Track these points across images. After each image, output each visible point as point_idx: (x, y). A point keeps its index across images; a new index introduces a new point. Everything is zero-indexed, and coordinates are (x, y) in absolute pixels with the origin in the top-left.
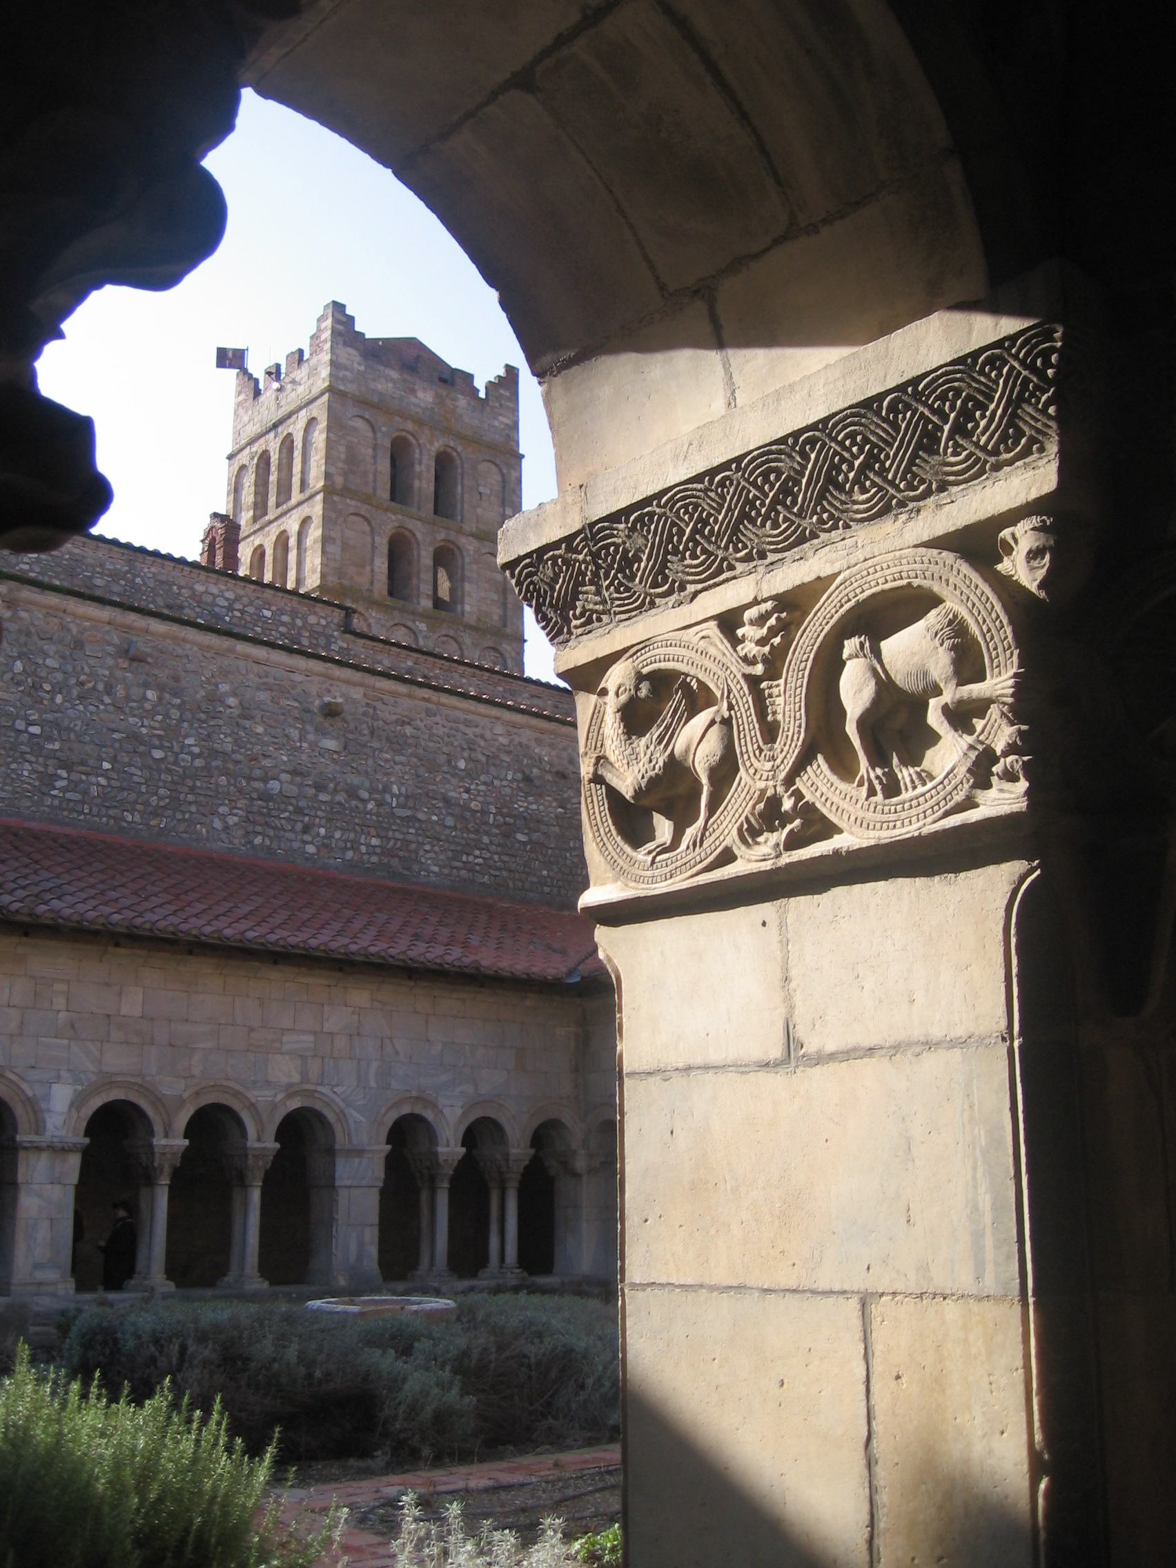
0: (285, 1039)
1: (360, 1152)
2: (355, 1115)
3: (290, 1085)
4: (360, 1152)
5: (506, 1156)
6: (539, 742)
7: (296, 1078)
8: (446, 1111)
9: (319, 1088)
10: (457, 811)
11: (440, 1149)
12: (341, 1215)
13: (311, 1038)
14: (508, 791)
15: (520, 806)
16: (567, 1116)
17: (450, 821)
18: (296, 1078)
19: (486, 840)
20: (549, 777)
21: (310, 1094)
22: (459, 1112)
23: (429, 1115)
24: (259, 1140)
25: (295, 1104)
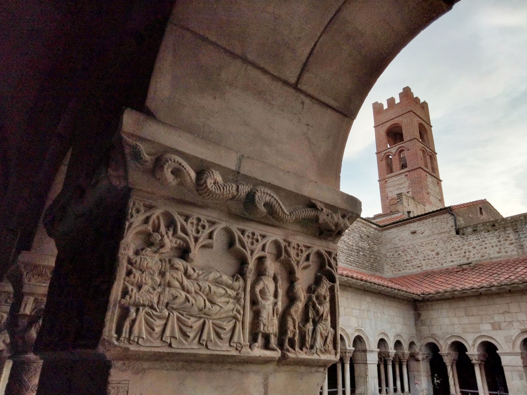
0: (353, 312)
1: (372, 351)
2: (371, 339)
3: (356, 327)
4: (372, 351)
5: (403, 354)
6: (362, 226)
7: (356, 325)
8: (390, 337)
9: (362, 329)
10: (347, 244)
11: (390, 351)
12: (369, 374)
13: (358, 311)
14: (357, 240)
15: (360, 244)
16: (415, 342)
17: (345, 247)
18: (356, 325)
19: (354, 253)
20: (366, 237)
21: (359, 330)
22: (393, 338)
23: (385, 338)
24: (349, 346)
25: (356, 334)
